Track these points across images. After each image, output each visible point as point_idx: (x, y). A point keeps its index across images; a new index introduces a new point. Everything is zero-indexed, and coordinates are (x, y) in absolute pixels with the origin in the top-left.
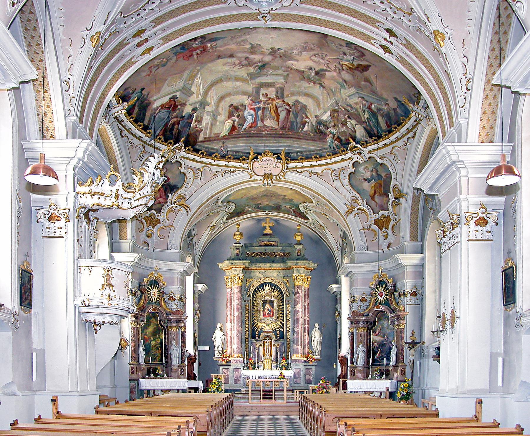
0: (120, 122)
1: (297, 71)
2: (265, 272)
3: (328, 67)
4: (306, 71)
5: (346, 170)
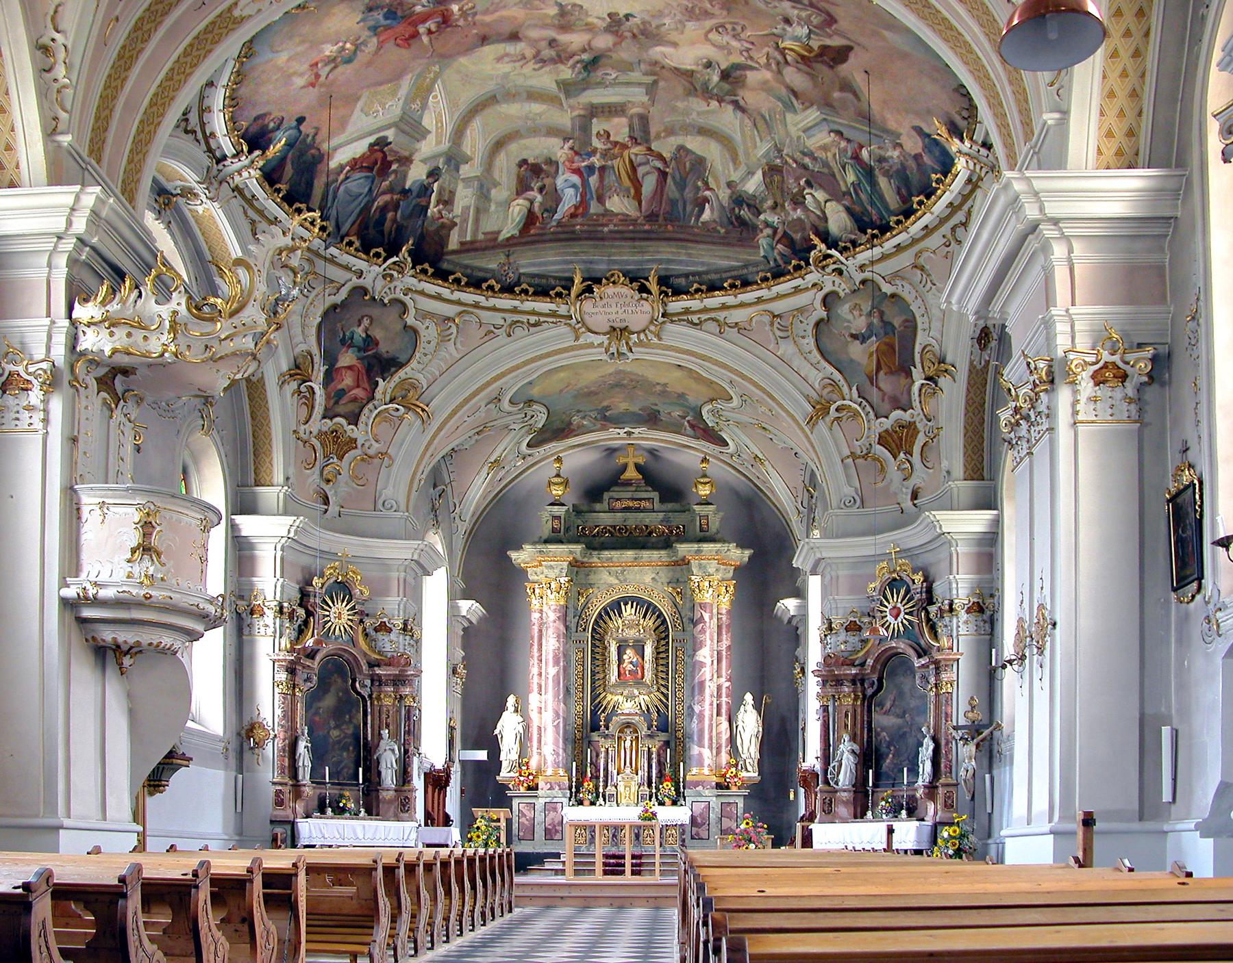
0: (250, 201)
1: (676, 70)
2: (622, 572)
3: (751, 58)
4: (698, 72)
5: (806, 314)
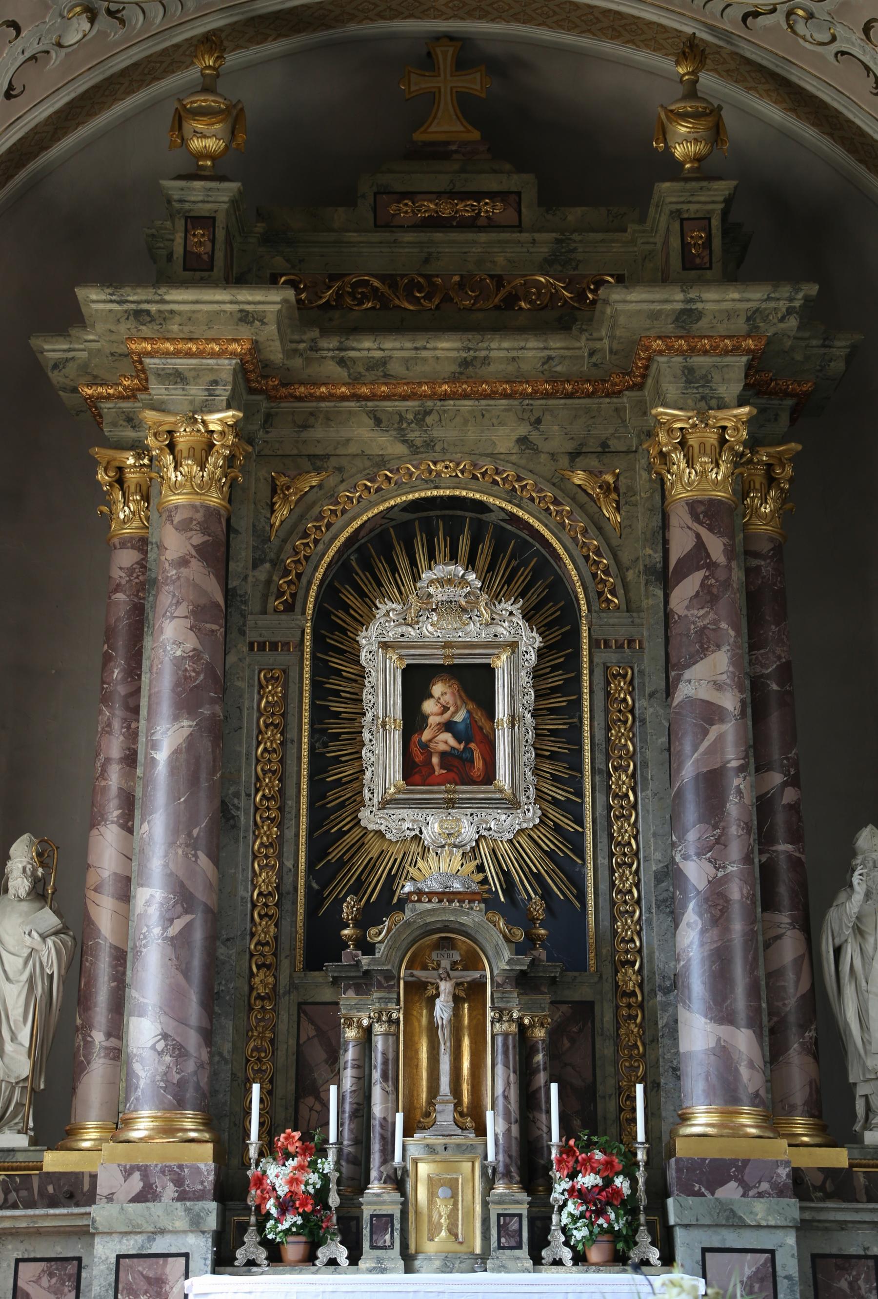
2: (421, 417)
